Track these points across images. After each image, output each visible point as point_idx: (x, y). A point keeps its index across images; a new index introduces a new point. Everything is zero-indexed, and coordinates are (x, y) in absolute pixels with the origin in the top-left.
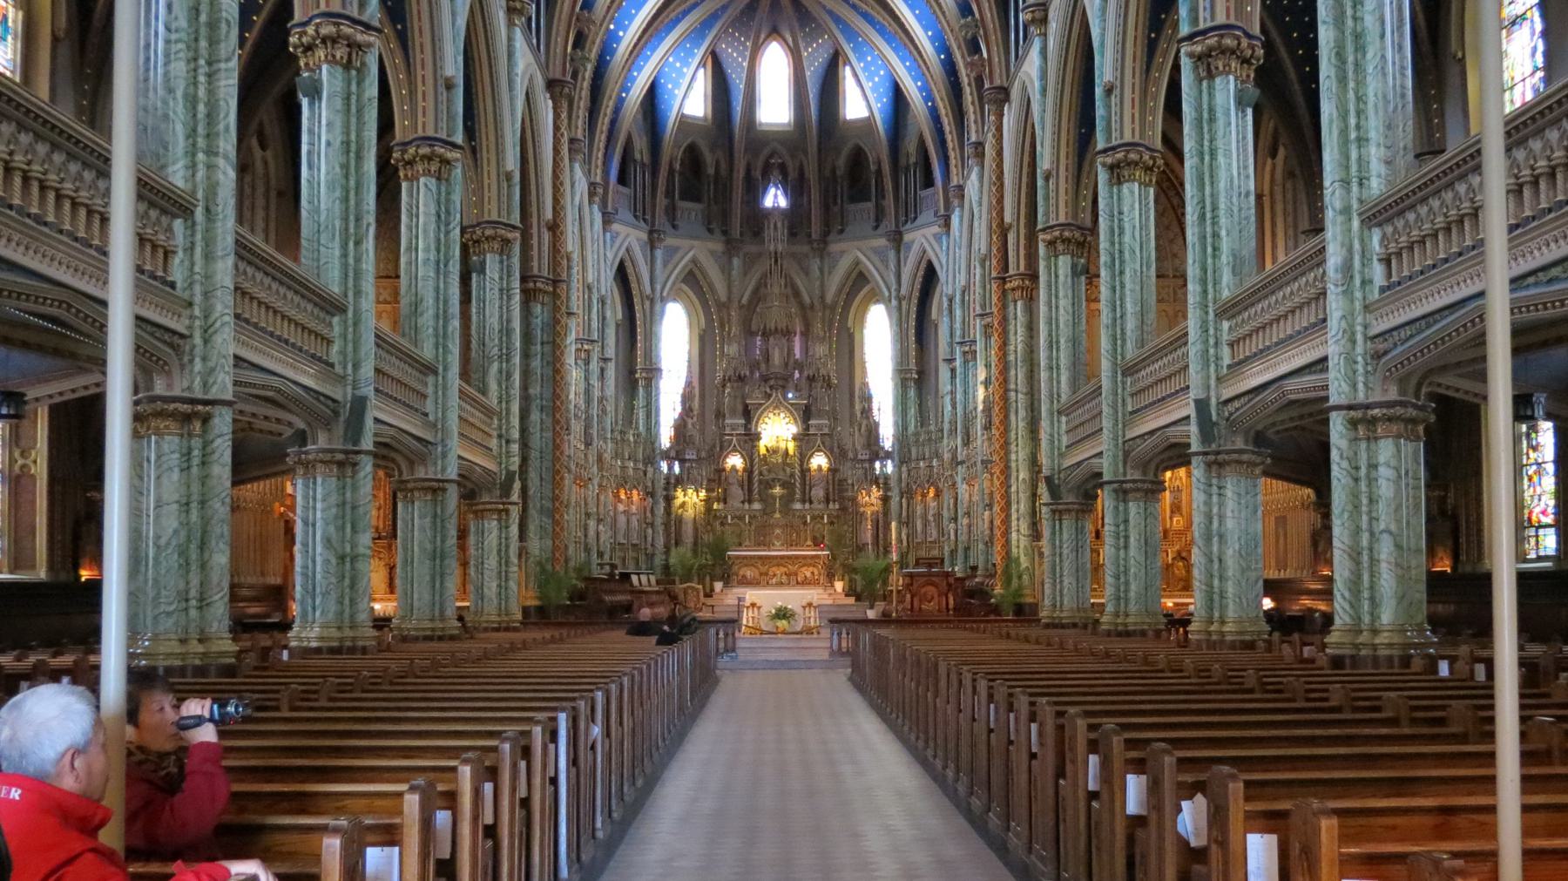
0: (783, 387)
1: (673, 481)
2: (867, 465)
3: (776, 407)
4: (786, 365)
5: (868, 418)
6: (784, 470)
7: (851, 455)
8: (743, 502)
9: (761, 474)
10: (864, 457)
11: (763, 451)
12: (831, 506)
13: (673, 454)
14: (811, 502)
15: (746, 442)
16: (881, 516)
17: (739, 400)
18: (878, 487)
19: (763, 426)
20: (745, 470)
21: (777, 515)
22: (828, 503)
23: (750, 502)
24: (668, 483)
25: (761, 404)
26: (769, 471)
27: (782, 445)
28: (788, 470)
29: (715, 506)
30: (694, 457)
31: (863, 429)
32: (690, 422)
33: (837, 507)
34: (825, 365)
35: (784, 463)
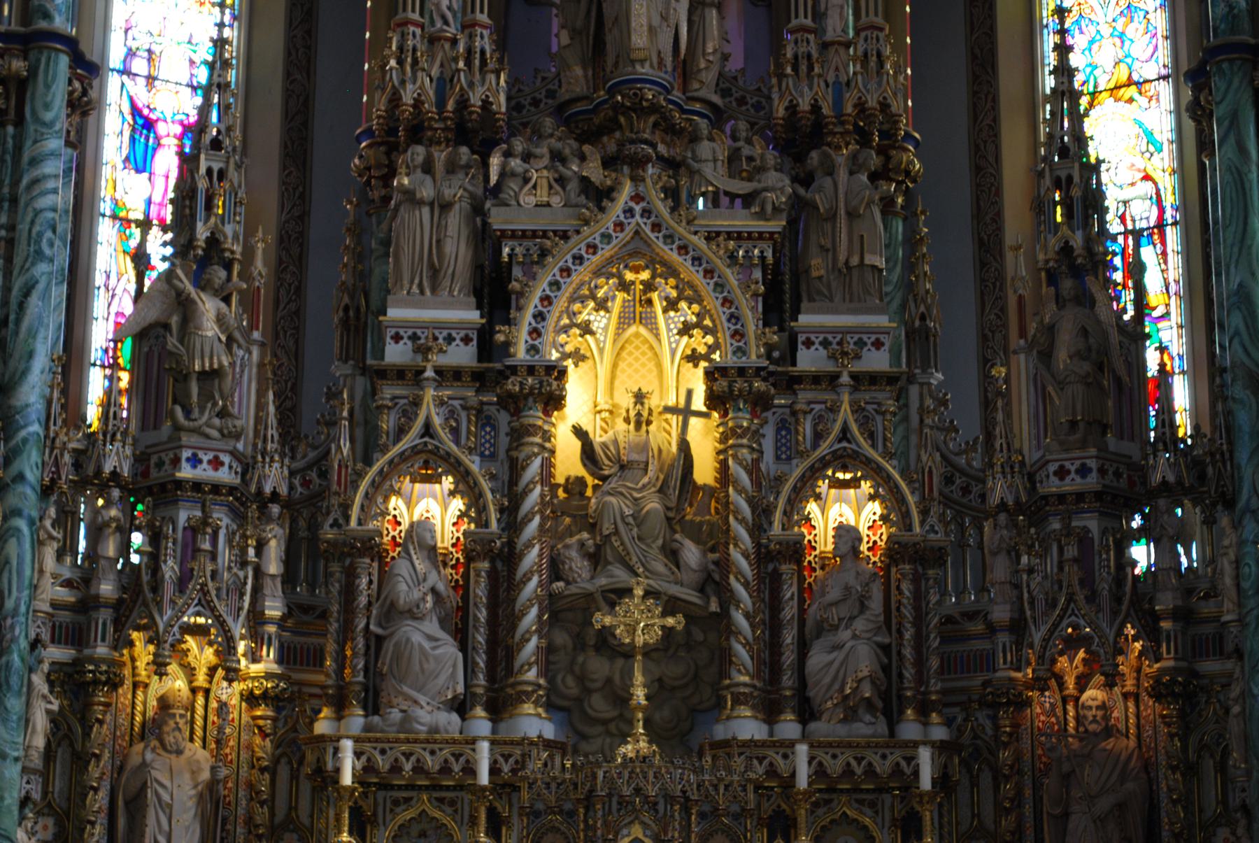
0: (672, 165)
1: (107, 588)
2: (1093, 524)
3: (637, 251)
4: (685, 69)
5: (1085, 300)
6: (672, 554)
7: (999, 489)
8: (461, 707)
9: (555, 569)
10: (1073, 484)
11: (568, 461)
12: (910, 729)
13: (116, 459)
14: (807, 713)
15: (482, 417)
16: (1168, 781)
17: (454, 221)
18: (1150, 632)
19: (573, 341)
20: (474, 548)
21: (637, 745)
22: (893, 723)
23: (499, 708)
24: (87, 604)
25: (565, 236)
26: (596, 559)
27: (663, 435)
28: (691, 553)
29: (322, 727)
30: (225, 476)
31: (1062, 356)
32: (209, 307)
33: (939, 733)
34: (873, 63)
35: (673, 520)
